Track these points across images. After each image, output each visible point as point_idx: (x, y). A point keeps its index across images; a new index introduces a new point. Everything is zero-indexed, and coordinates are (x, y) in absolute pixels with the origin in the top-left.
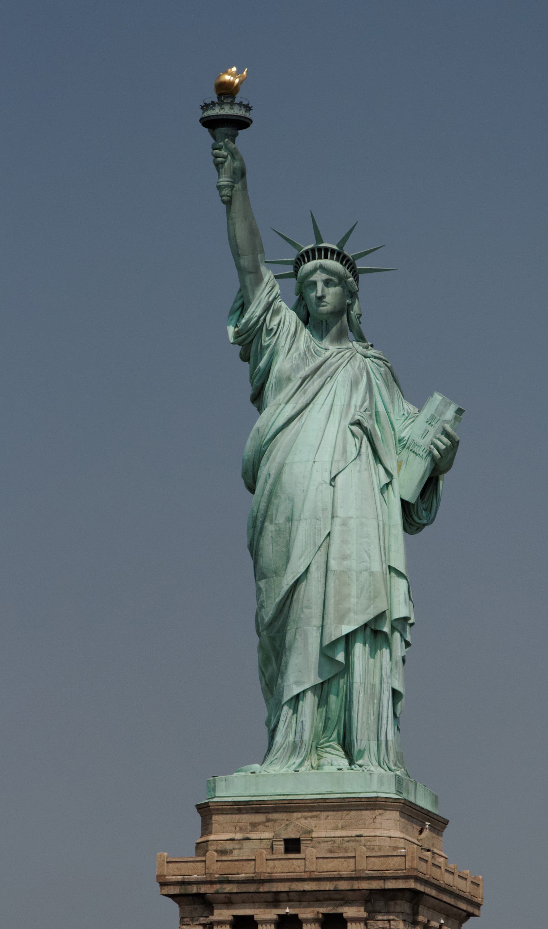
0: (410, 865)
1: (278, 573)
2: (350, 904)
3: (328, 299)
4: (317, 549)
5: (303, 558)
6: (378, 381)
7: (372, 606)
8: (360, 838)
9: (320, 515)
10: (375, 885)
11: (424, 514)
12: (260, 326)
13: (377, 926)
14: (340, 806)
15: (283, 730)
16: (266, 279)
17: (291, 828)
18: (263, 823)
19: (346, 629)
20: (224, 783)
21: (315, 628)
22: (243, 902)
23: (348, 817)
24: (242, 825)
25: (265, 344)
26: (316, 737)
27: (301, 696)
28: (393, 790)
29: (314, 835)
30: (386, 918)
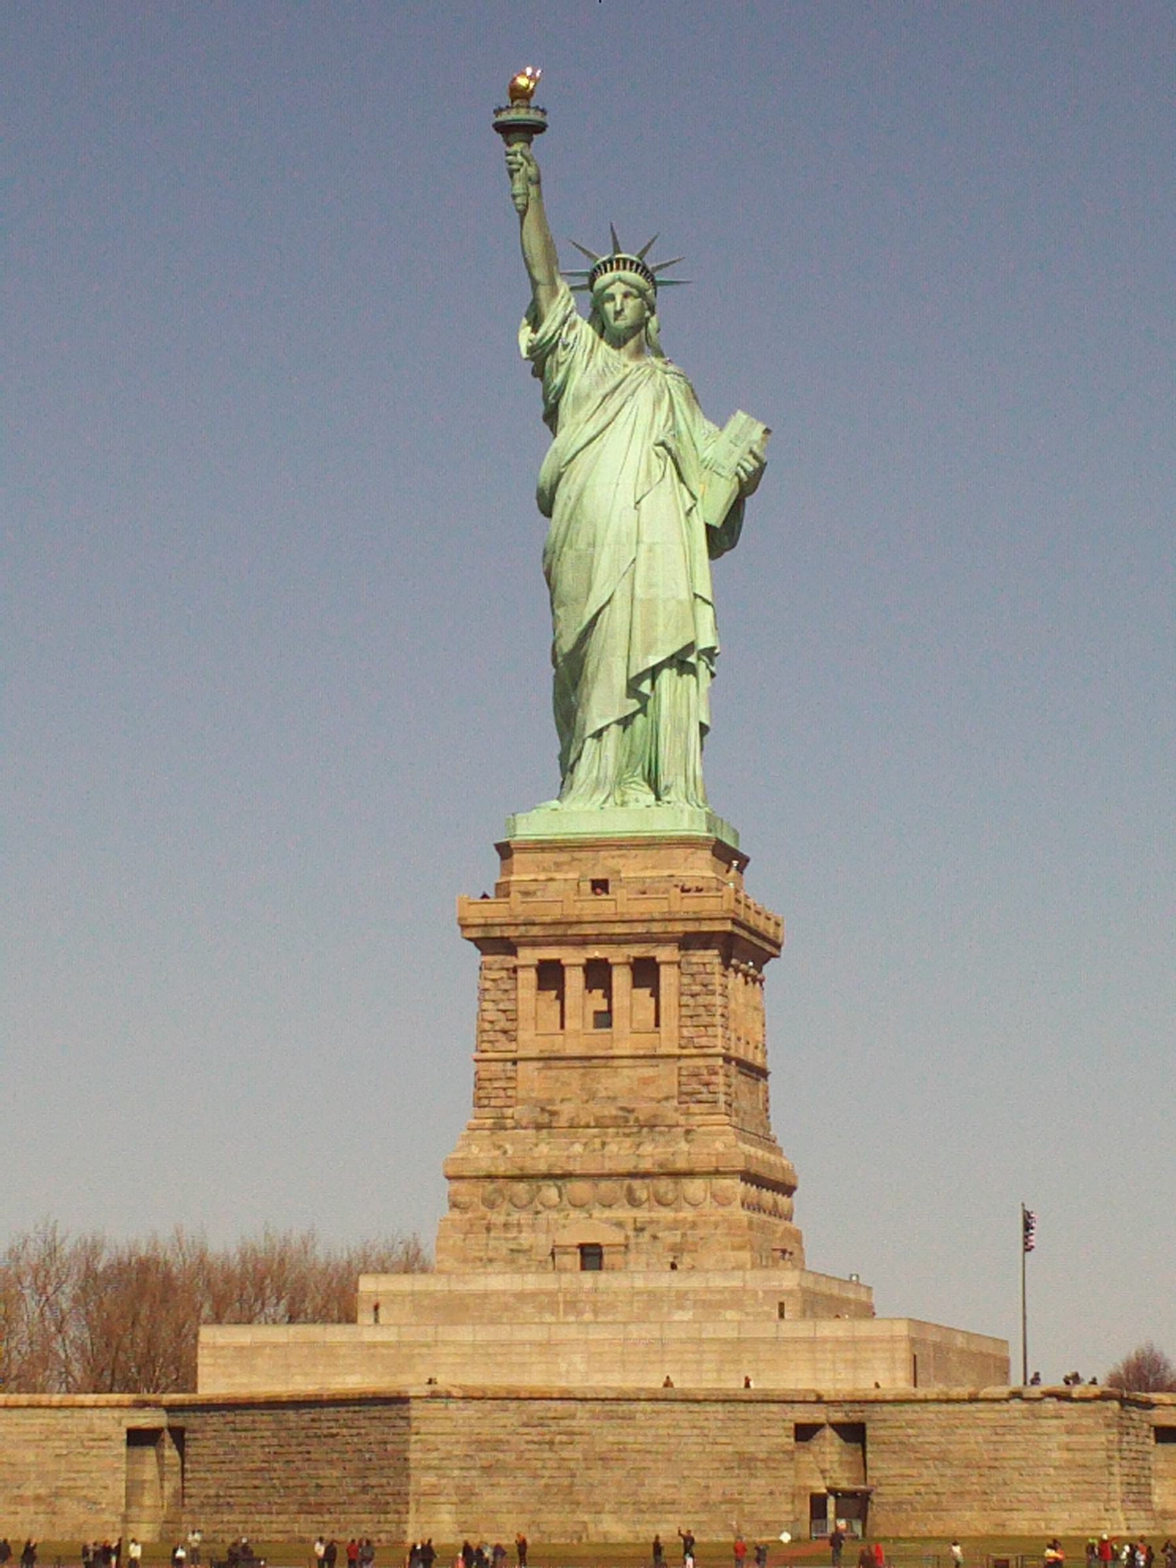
3: (627, 312)
4: (621, 574)
9: (624, 540)
10: (691, 927)
14: (649, 845)
16: (561, 292)
17: (598, 868)
19: (653, 661)
20: (525, 820)
21: (620, 659)
25: (561, 360)
26: (619, 774)
28: (705, 828)
29: (623, 875)
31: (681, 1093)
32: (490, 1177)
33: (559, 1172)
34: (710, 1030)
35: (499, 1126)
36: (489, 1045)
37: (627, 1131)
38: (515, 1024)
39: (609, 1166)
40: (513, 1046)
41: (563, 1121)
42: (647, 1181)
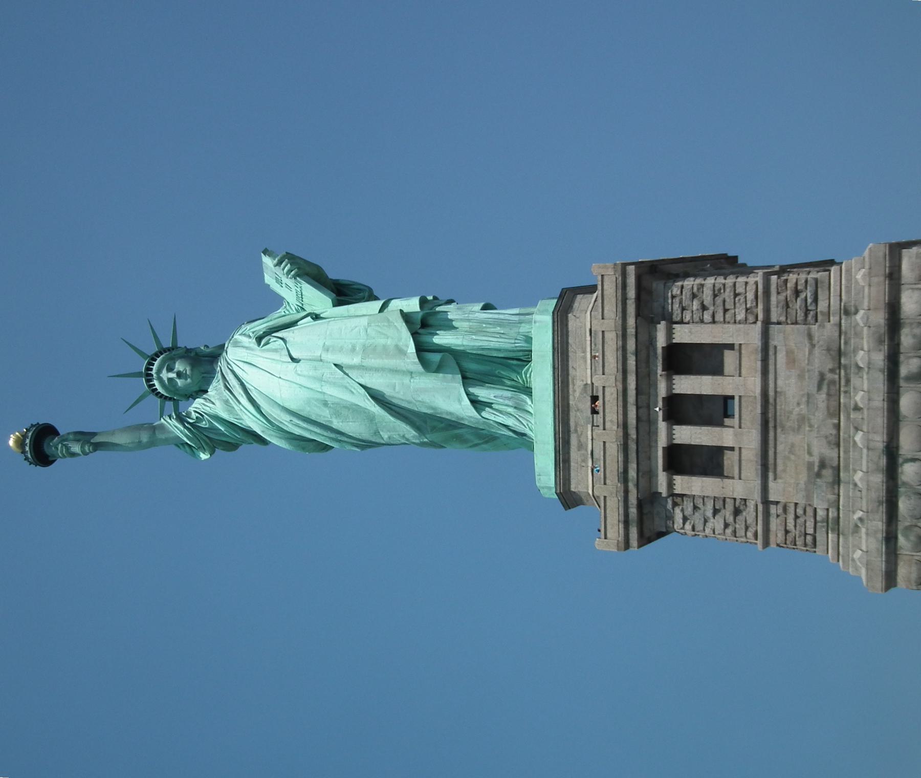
0: (610, 270)
1: (371, 418)
2: (654, 340)
4: (346, 376)
5: (353, 390)
6: (248, 329)
7: (395, 324)
8: (593, 332)
9: (318, 373)
11: (361, 294)
12: (191, 426)
13: (677, 310)
15: (503, 418)
17: (581, 406)
18: (579, 437)
19: (412, 348)
20: (541, 477)
22: (649, 458)
23: (574, 346)
24: (579, 460)
27: (472, 397)
30: (670, 301)
31: (805, 322)
32: (890, 539)
33: (883, 461)
34: (740, 290)
35: (835, 525)
36: (750, 529)
37: (843, 382)
38: (728, 500)
39: (879, 401)
40: (751, 505)
41: (831, 453)
42: (902, 358)
